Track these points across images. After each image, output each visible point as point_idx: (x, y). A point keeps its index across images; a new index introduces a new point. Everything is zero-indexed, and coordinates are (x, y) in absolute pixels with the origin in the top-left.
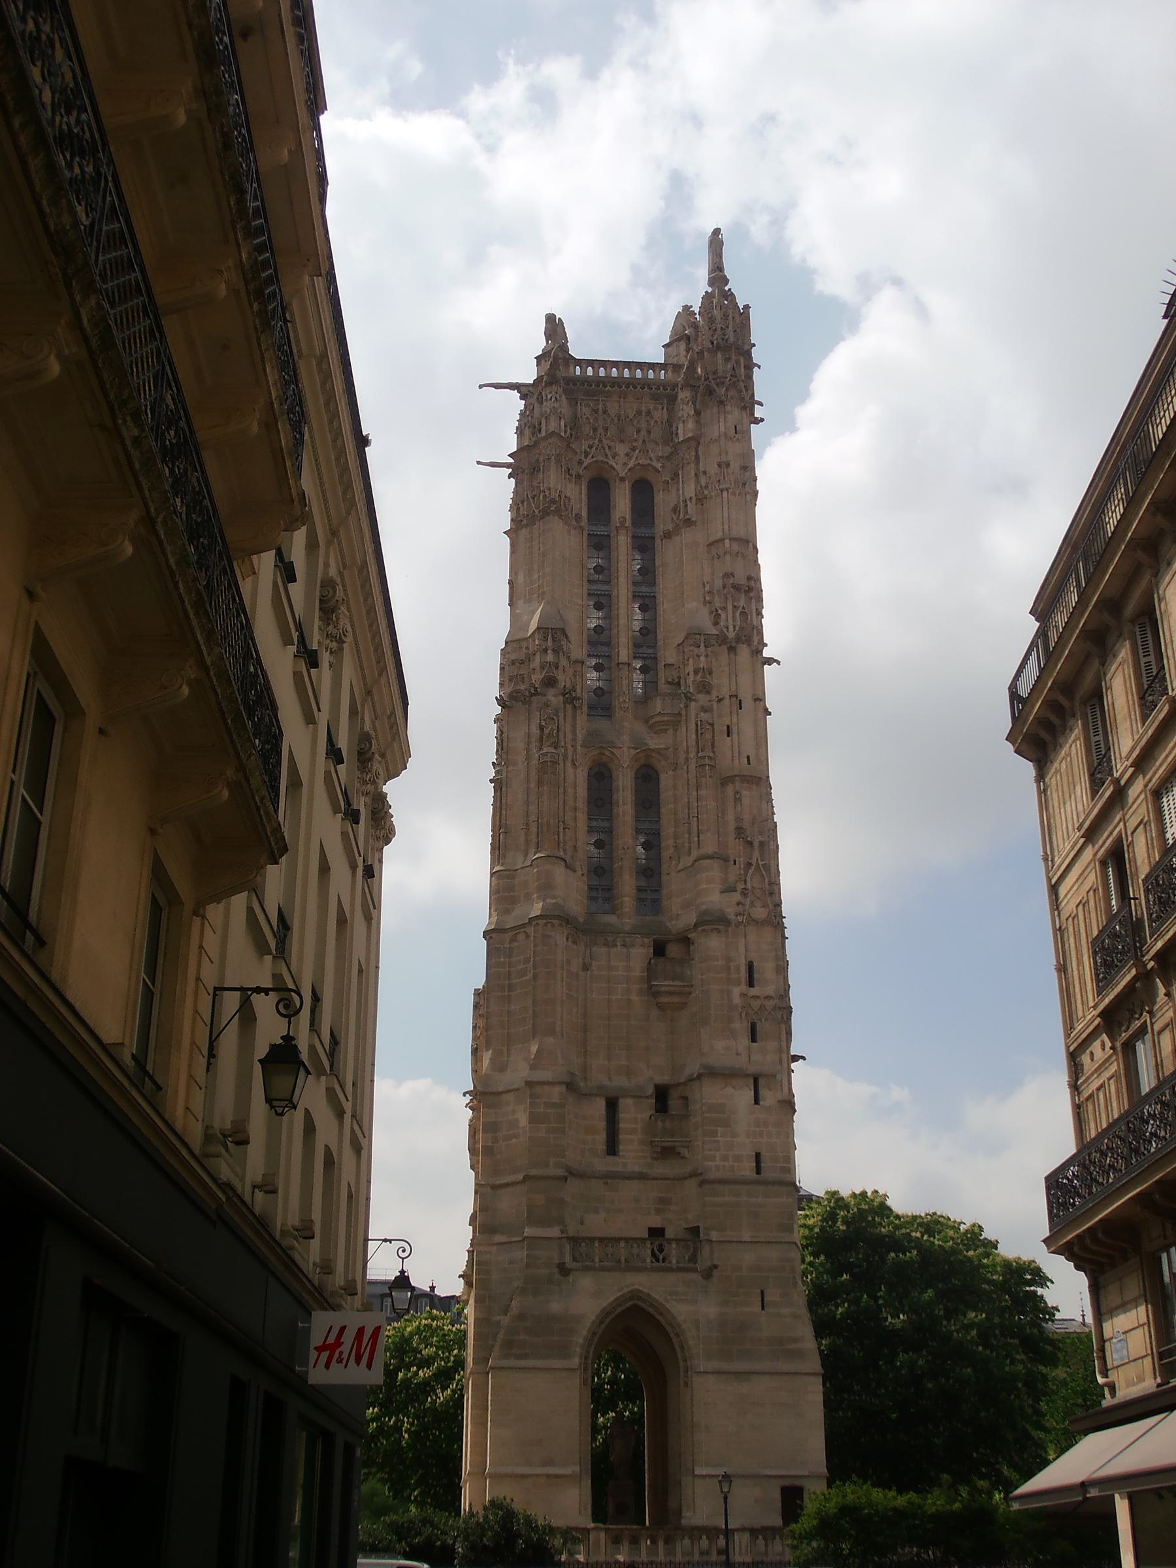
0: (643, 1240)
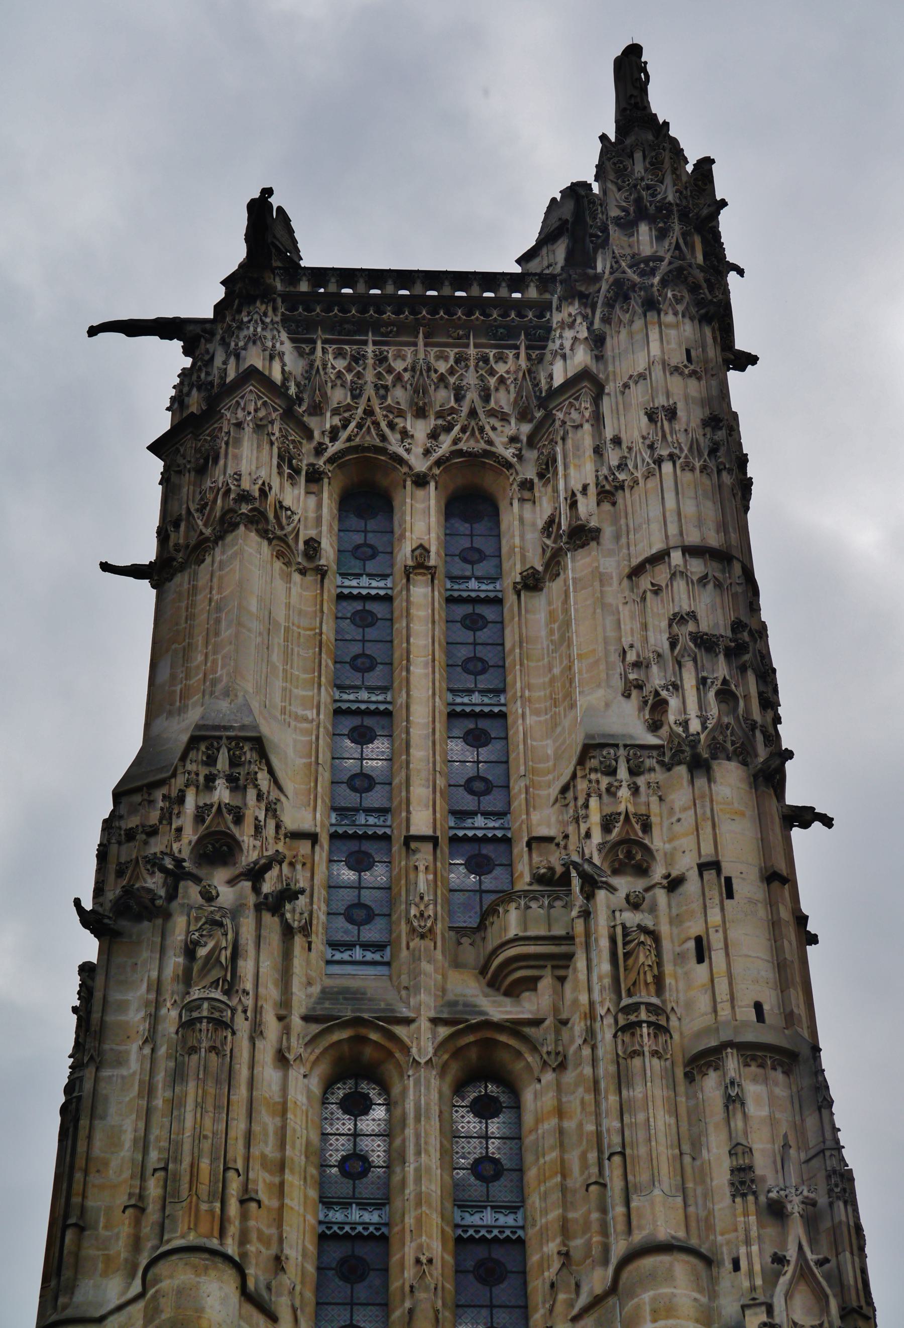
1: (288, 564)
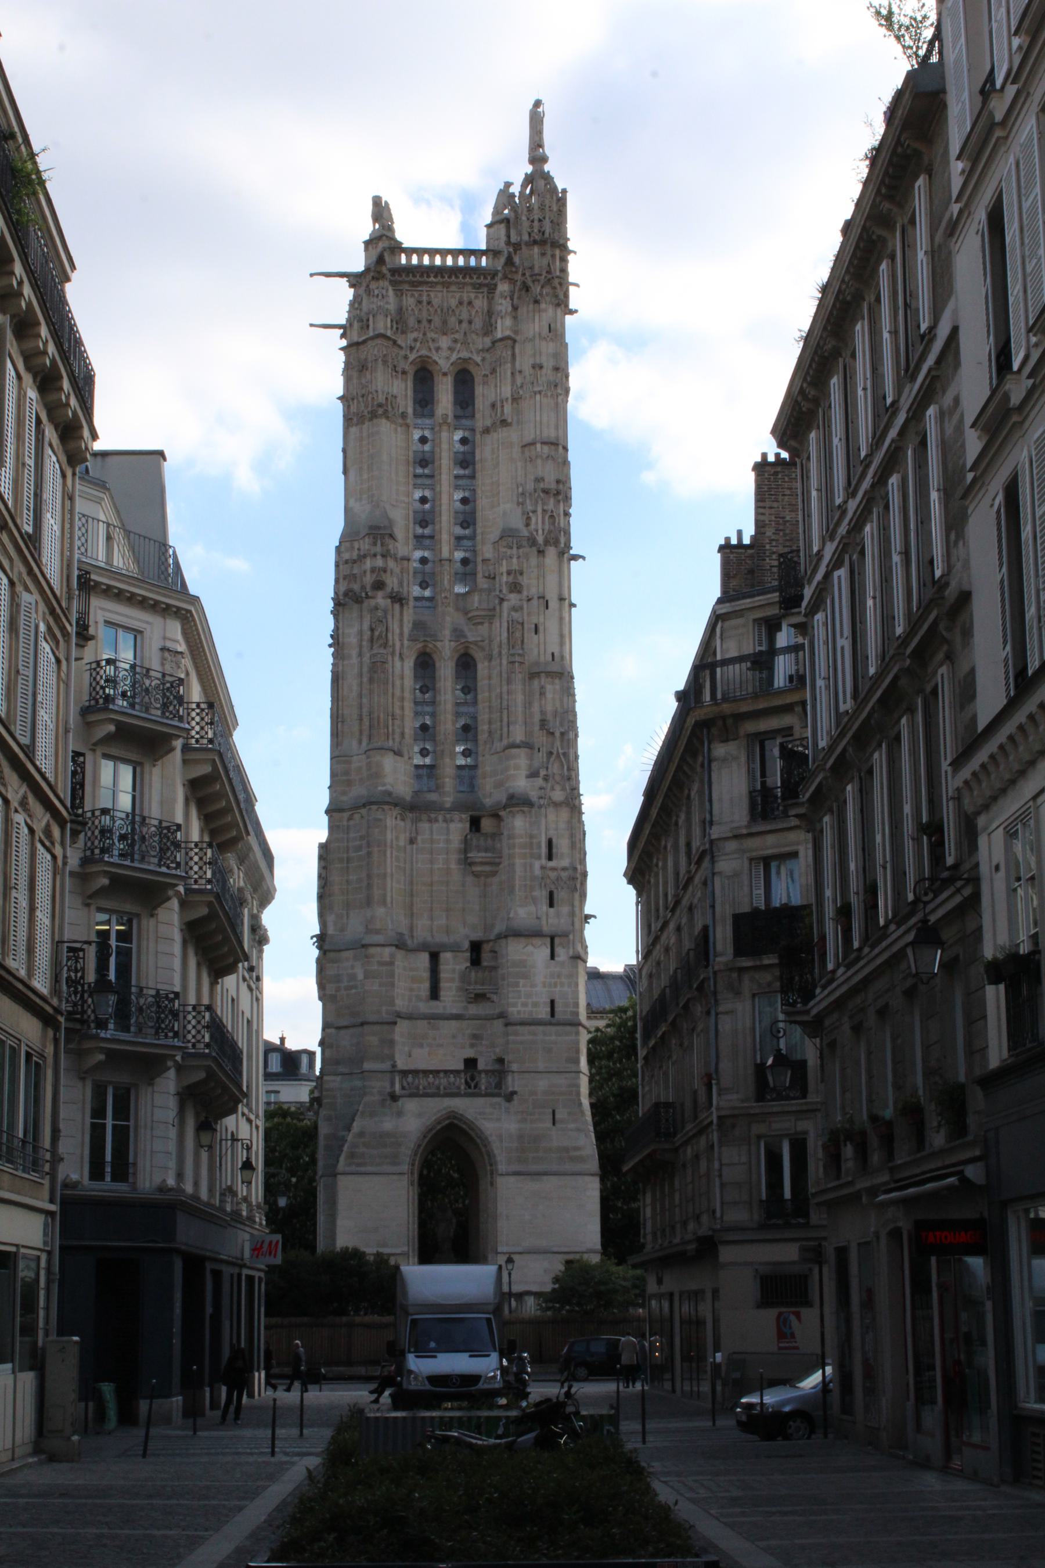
0: (456, 1072)
1: (396, 424)
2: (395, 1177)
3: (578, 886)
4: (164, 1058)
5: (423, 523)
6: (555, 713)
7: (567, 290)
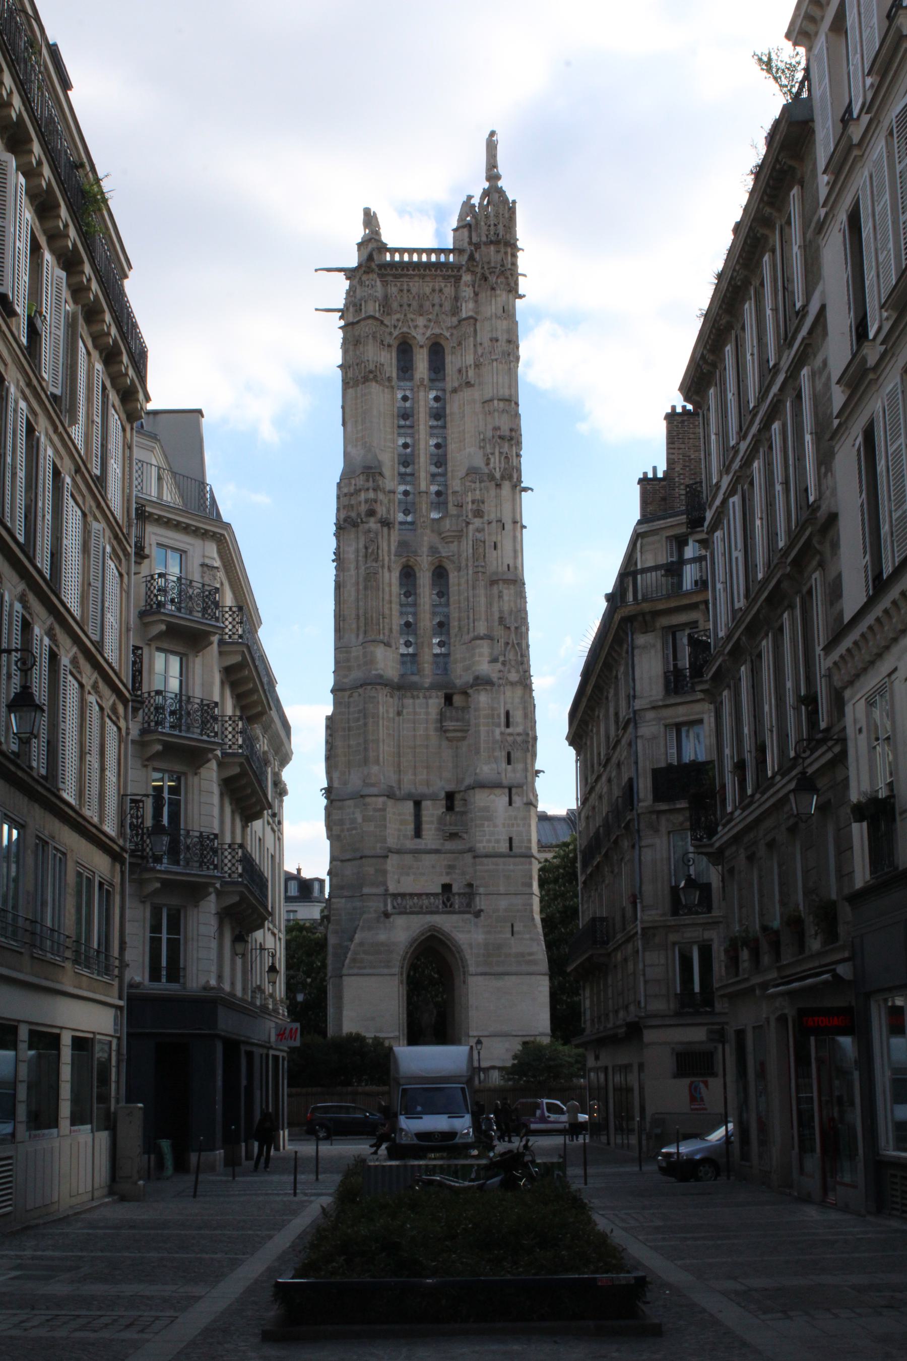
2: (389, 978)
3: (530, 748)
4: (206, 885)
5: (406, 464)
6: (511, 612)
7: (517, 279)
